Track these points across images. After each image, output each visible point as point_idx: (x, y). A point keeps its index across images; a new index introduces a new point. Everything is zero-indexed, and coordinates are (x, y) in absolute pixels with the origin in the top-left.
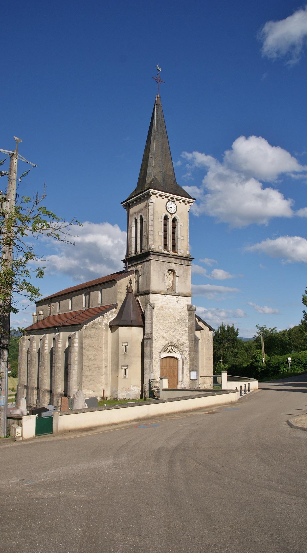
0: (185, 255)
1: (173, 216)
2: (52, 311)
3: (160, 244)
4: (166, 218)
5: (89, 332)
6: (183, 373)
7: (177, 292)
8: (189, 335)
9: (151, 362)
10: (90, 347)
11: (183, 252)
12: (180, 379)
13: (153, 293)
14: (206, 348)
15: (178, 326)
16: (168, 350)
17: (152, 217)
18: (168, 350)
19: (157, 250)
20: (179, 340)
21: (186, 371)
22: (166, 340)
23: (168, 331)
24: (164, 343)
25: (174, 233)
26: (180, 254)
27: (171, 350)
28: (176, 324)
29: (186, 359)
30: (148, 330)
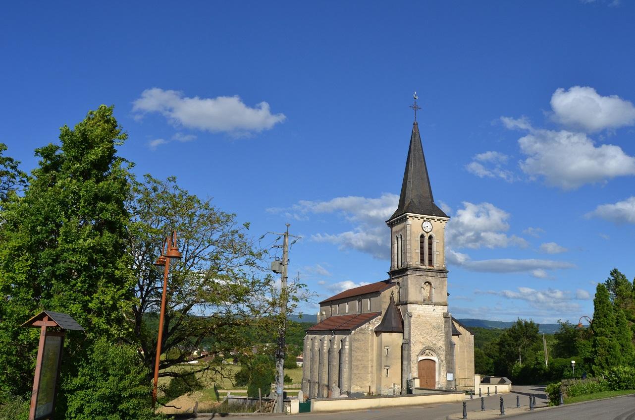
0: (441, 268)
2: (333, 312)
3: (417, 260)
4: (422, 236)
5: (357, 336)
6: (439, 374)
7: (433, 301)
8: (445, 340)
9: (409, 364)
10: (358, 349)
11: (438, 265)
12: (437, 380)
13: (411, 303)
14: (467, 351)
15: (434, 332)
16: (426, 354)
17: (409, 237)
18: (426, 354)
19: (414, 266)
20: (435, 344)
21: (443, 373)
22: (424, 345)
23: (425, 337)
25: (430, 249)
26: (436, 268)
29: (442, 361)
30: (406, 336)
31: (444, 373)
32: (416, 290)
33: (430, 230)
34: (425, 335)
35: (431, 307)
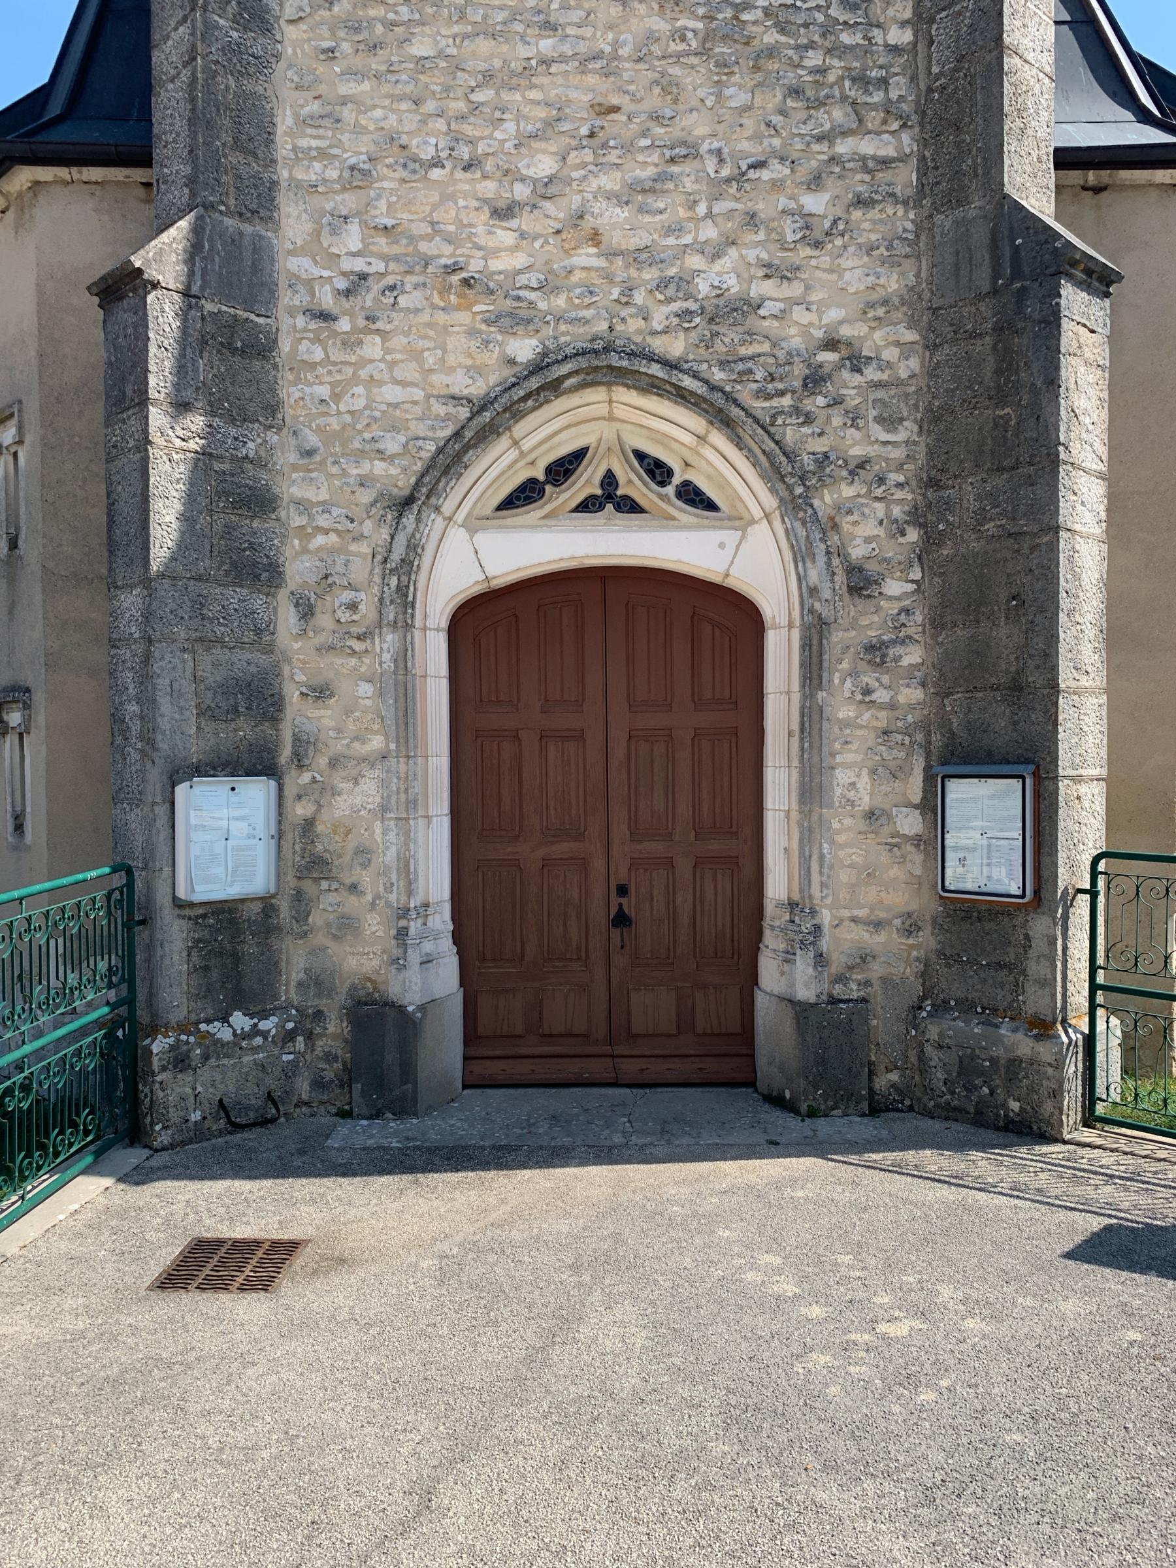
6: (812, 790)
12: (778, 883)
16: (586, 482)
18: (586, 482)
22: (517, 319)
23: (546, 190)
24: (467, 359)
27: (633, 484)
28: (695, 80)
29: (861, 583)
31: (880, 771)
34: (543, 165)
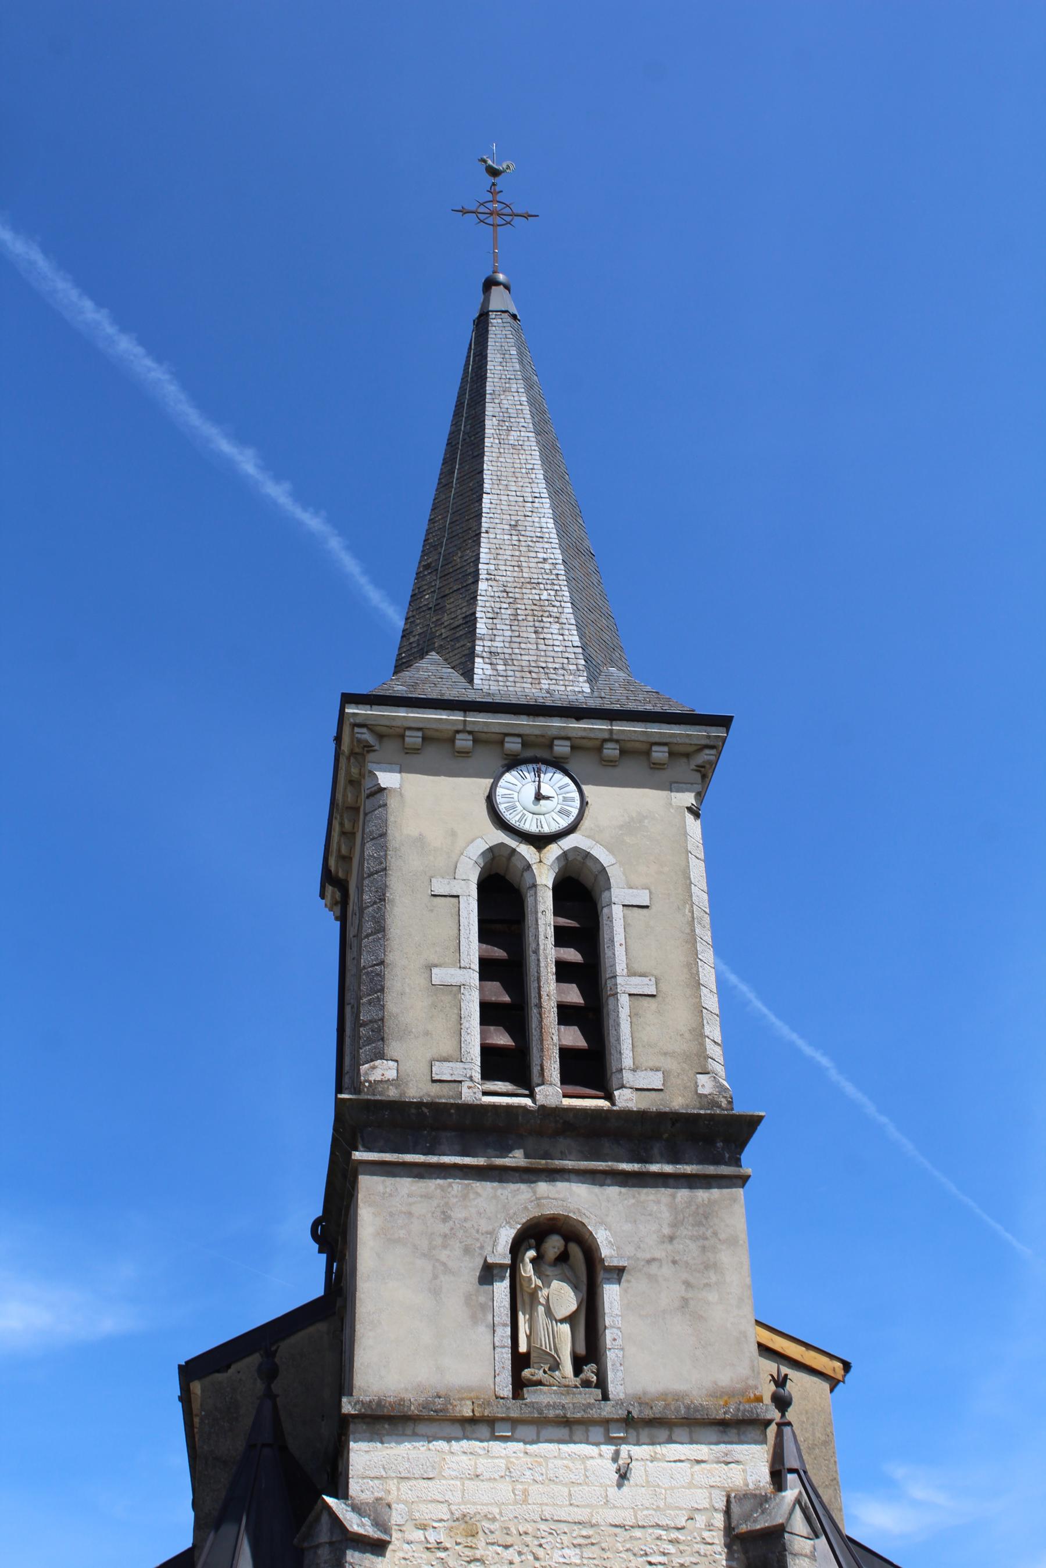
0: (678, 1102)
1: (553, 851)
3: (446, 1047)
7: (615, 1389)
11: (655, 1080)
19: (417, 1090)
25: (588, 972)
26: (625, 1099)
32: (436, 1292)
33: (564, 823)
35: (593, 1458)
